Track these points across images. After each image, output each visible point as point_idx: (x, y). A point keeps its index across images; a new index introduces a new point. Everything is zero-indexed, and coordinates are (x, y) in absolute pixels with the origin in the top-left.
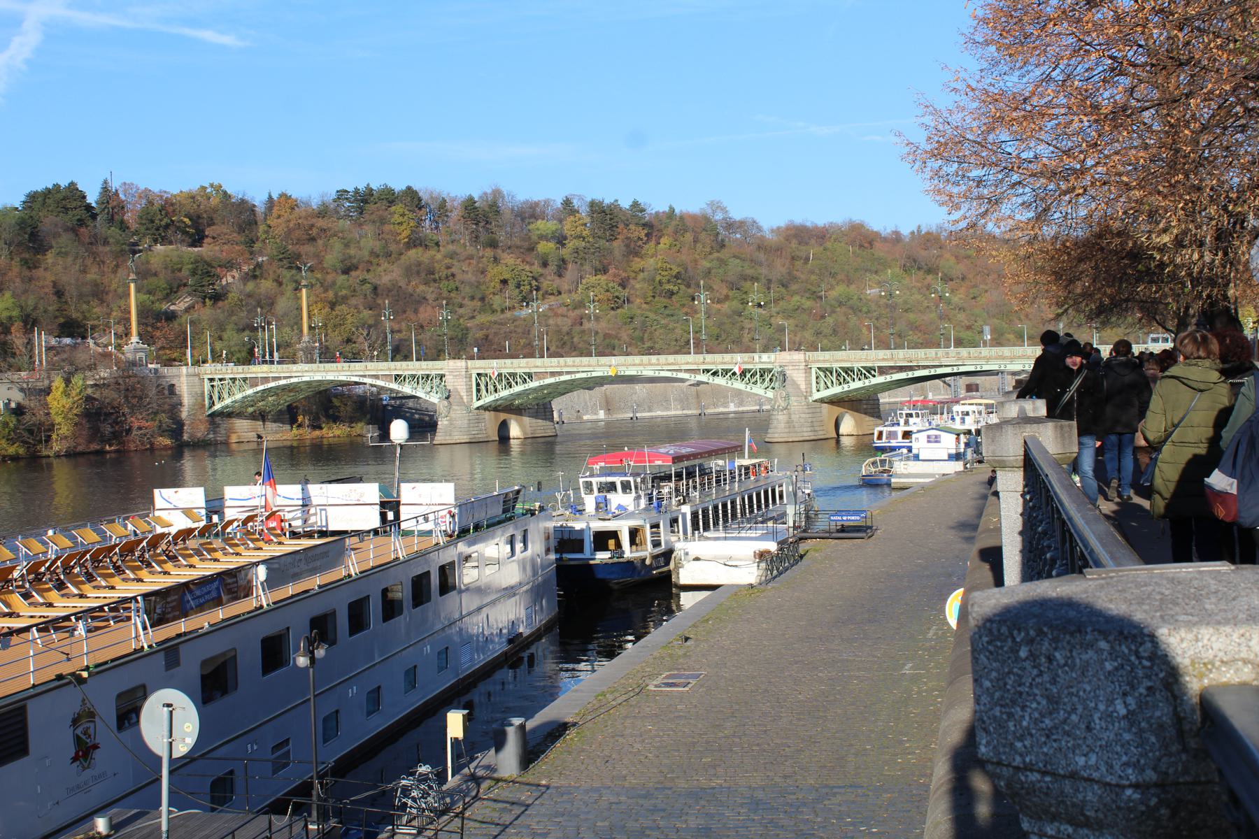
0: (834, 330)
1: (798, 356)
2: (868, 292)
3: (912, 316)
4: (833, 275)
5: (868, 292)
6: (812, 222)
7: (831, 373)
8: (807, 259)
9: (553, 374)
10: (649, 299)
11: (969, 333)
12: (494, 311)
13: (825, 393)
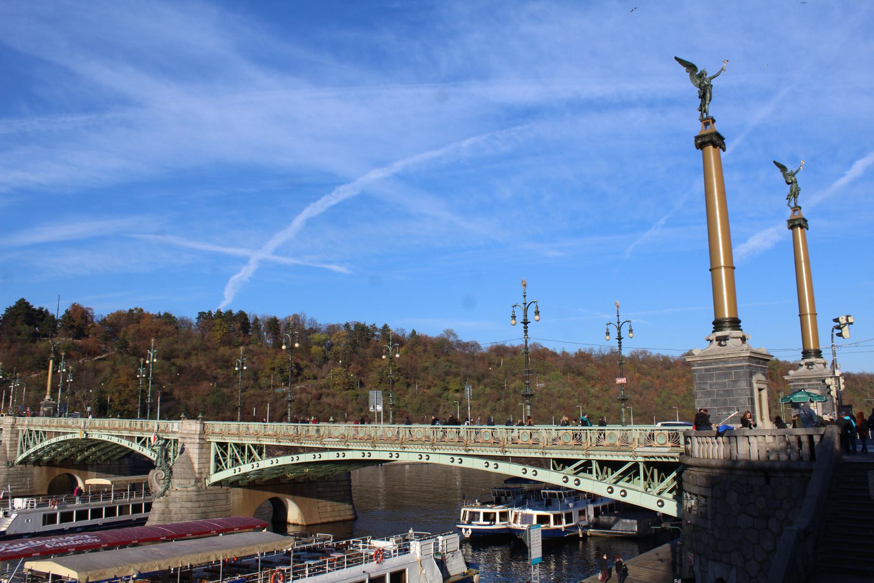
0: (506, 408)
1: (192, 427)
2: (538, 385)
3: (561, 400)
4: (514, 375)
5: (538, 385)
6: (511, 344)
7: (243, 450)
8: (499, 364)
9: (58, 434)
10: (377, 385)
11: (599, 412)
12: (261, 388)
13: (228, 473)
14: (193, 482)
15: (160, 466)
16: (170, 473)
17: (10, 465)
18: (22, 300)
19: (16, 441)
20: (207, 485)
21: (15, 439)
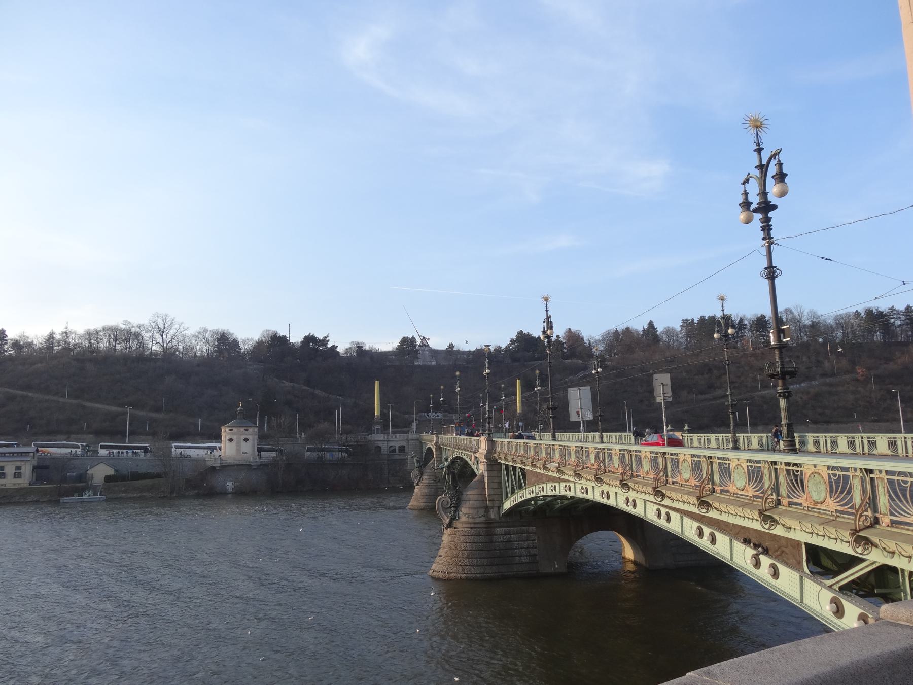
14: (482, 512)
15: (448, 492)
16: (456, 501)
17: (437, 480)
18: (521, 333)
19: (440, 457)
20: (501, 516)
21: (440, 456)
